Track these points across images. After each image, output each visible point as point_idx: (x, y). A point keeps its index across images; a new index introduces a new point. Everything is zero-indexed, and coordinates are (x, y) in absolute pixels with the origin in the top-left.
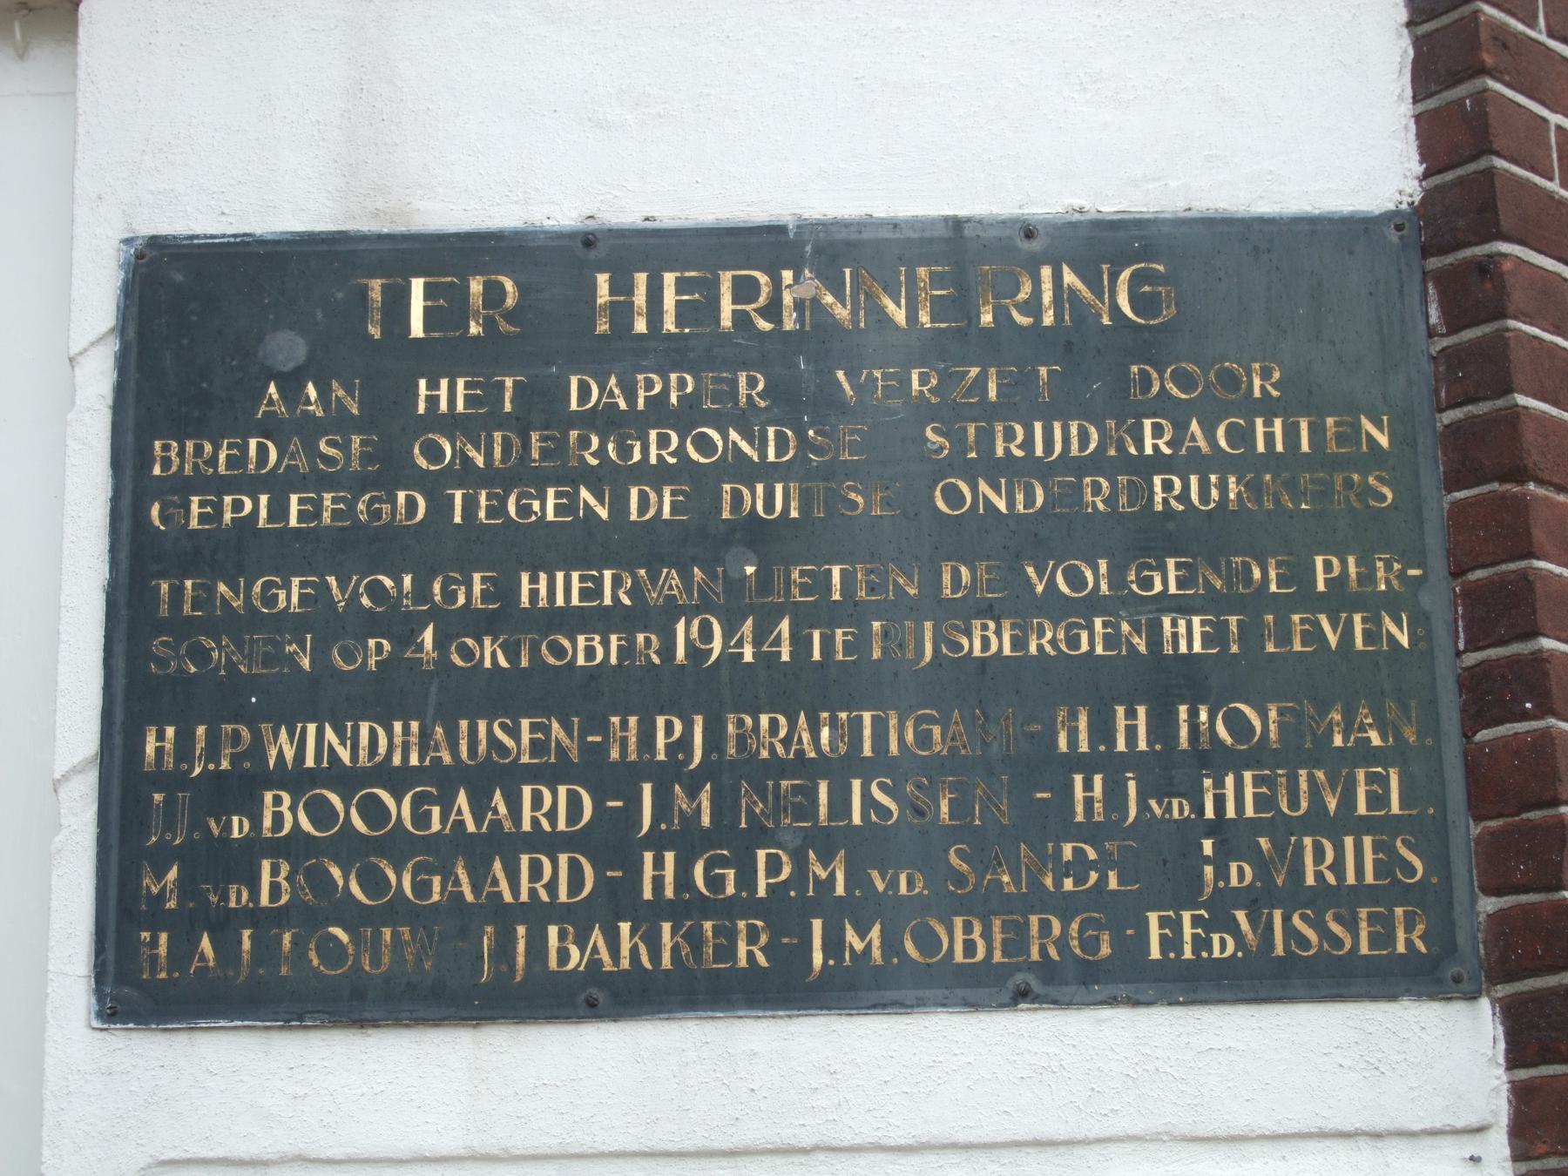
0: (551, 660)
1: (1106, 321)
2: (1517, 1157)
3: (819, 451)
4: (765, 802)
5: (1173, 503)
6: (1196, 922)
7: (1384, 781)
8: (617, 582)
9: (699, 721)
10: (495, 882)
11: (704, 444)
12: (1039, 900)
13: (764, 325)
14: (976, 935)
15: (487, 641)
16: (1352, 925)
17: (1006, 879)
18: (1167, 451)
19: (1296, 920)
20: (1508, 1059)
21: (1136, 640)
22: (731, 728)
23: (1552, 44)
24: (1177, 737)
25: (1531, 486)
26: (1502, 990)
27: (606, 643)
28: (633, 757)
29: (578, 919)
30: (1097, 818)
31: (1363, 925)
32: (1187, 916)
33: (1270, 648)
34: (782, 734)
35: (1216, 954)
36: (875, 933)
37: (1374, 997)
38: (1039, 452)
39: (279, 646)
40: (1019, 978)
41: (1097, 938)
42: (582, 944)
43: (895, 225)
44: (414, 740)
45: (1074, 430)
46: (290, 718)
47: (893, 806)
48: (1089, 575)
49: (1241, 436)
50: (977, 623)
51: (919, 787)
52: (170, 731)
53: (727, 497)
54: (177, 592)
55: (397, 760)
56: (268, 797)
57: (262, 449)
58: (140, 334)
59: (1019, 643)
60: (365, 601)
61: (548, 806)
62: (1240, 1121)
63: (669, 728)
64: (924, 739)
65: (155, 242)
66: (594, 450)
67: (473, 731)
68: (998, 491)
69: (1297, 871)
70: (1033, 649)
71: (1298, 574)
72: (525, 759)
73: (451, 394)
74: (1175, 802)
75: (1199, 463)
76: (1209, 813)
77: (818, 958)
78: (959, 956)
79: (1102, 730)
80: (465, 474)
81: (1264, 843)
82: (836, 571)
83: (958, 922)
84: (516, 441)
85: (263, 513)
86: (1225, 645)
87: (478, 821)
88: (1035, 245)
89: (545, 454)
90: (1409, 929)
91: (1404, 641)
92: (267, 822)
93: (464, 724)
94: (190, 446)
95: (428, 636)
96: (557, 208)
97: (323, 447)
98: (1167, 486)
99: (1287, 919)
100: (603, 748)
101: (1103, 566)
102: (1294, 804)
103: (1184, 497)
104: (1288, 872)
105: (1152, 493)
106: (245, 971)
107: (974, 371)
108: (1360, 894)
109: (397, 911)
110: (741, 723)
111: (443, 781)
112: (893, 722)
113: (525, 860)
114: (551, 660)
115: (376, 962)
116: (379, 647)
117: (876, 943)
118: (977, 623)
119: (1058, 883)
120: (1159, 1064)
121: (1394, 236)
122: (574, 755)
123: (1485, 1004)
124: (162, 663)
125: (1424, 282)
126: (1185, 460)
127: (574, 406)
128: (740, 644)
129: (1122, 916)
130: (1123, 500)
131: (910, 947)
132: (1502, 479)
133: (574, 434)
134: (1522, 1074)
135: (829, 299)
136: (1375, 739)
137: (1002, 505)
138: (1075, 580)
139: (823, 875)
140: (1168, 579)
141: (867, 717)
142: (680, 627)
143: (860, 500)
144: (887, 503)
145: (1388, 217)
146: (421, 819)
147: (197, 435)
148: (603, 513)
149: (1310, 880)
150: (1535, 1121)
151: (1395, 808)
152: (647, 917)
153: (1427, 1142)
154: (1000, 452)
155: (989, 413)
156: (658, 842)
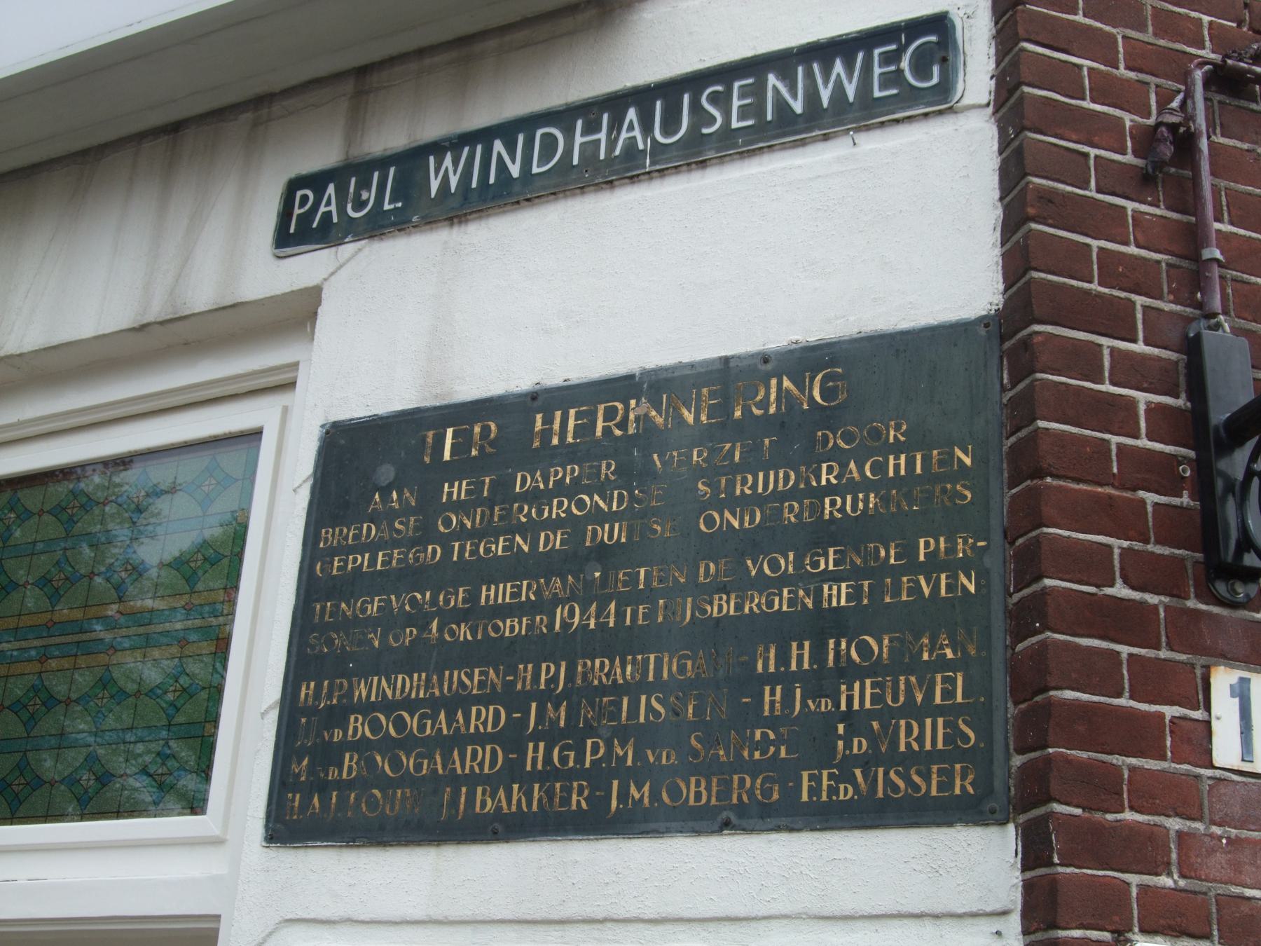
0: (493, 634)
1: (805, 407)
2: (1025, 932)
3: (639, 502)
4: (593, 710)
5: (836, 513)
6: (831, 776)
7: (953, 681)
8: (529, 587)
9: (563, 664)
10: (454, 763)
11: (581, 505)
12: (739, 765)
13: (618, 433)
14: (702, 789)
15: (463, 626)
16: (927, 777)
17: (721, 753)
18: (834, 482)
19: (892, 775)
20: (1023, 865)
21: (807, 600)
22: (580, 668)
23: (1100, 197)
24: (827, 659)
25: (1049, 480)
26: (1022, 818)
27: (520, 623)
28: (528, 688)
29: (492, 783)
30: (776, 713)
31: (934, 776)
32: (825, 773)
33: (888, 600)
34: (606, 670)
35: (841, 797)
36: (646, 788)
37: (939, 824)
38: (760, 490)
39: (365, 635)
40: (725, 815)
41: (771, 789)
42: (493, 797)
43: (692, 365)
44: (422, 683)
45: (781, 475)
46: (365, 675)
47: (662, 710)
48: (782, 562)
49: (880, 468)
50: (716, 597)
51: (677, 698)
52: (312, 684)
53: (589, 534)
54: (323, 608)
55: (413, 695)
56: (352, 718)
57: (369, 529)
58: (323, 474)
59: (739, 607)
60: (407, 608)
61: (484, 718)
62: (848, 906)
63: (548, 668)
64: (682, 669)
65: (336, 425)
66: (526, 512)
67: (451, 676)
68: (734, 516)
69: (895, 742)
70: (747, 610)
71: (908, 551)
72: (475, 692)
73: (458, 490)
74: (823, 701)
75: (853, 487)
76: (843, 707)
77: (614, 803)
78: (692, 802)
79: (783, 658)
80: (461, 534)
81: (875, 725)
82: (642, 571)
83: (693, 780)
84: (488, 512)
85: (366, 563)
86: (860, 599)
87: (449, 727)
88: (769, 367)
89: (501, 518)
90: (963, 778)
91: (972, 589)
92: (350, 732)
93: (447, 673)
94: (337, 530)
95: (435, 625)
96: (520, 381)
97: (397, 525)
98: (833, 503)
99: (886, 774)
100: (514, 683)
101: (791, 556)
102: (895, 699)
103: (842, 510)
104: (889, 743)
105: (823, 508)
106: (332, 815)
107: (728, 446)
108: (935, 756)
109: (405, 780)
110: (585, 665)
111: (435, 704)
112: (666, 659)
113: (469, 748)
114: (493, 634)
115: (392, 809)
116: (411, 632)
117: (647, 794)
118: (716, 597)
119: (751, 755)
120: (803, 869)
121: (982, 331)
122: (499, 688)
123: (1011, 828)
124: (313, 647)
125: (1001, 358)
126: (843, 486)
127: (518, 490)
128: (588, 619)
129: (786, 774)
130: (806, 514)
131: (665, 796)
132: (1032, 478)
133: (516, 505)
134: (1029, 875)
135: (654, 413)
136: (949, 653)
137: (736, 524)
138: (774, 566)
139: (621, 753)
140: (828, 562)
141: (652, 657)
142: (559, 611)
143: (659, 528)
144: (673, 529)
145: (984, 321)
146: (422, 728)
147: (341, 524)
148: (526, 548)
149: (902, 748)
150: (1042, 907)
151: (959, 699)
152: (526, 780)
153: (970, 921)
154: (738, 492)
155: (735, 469)
156: (536, 737)
